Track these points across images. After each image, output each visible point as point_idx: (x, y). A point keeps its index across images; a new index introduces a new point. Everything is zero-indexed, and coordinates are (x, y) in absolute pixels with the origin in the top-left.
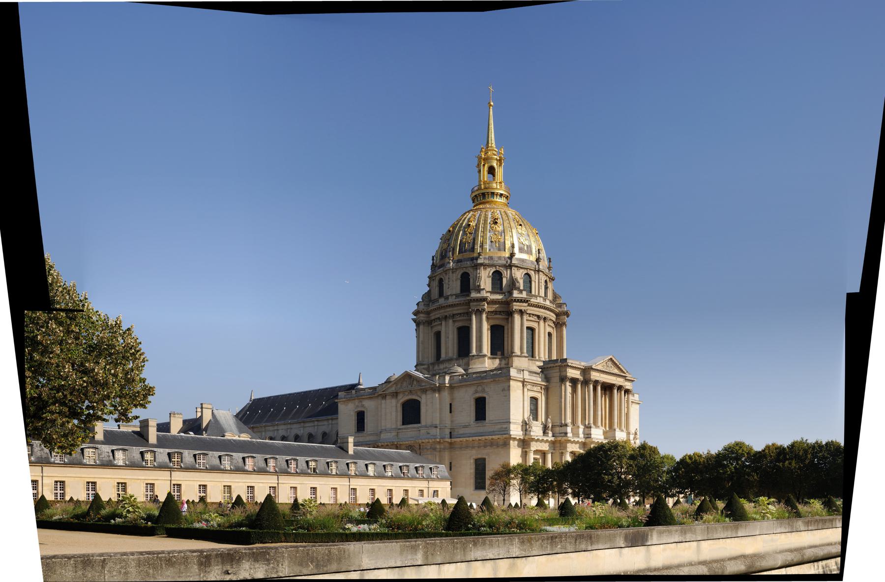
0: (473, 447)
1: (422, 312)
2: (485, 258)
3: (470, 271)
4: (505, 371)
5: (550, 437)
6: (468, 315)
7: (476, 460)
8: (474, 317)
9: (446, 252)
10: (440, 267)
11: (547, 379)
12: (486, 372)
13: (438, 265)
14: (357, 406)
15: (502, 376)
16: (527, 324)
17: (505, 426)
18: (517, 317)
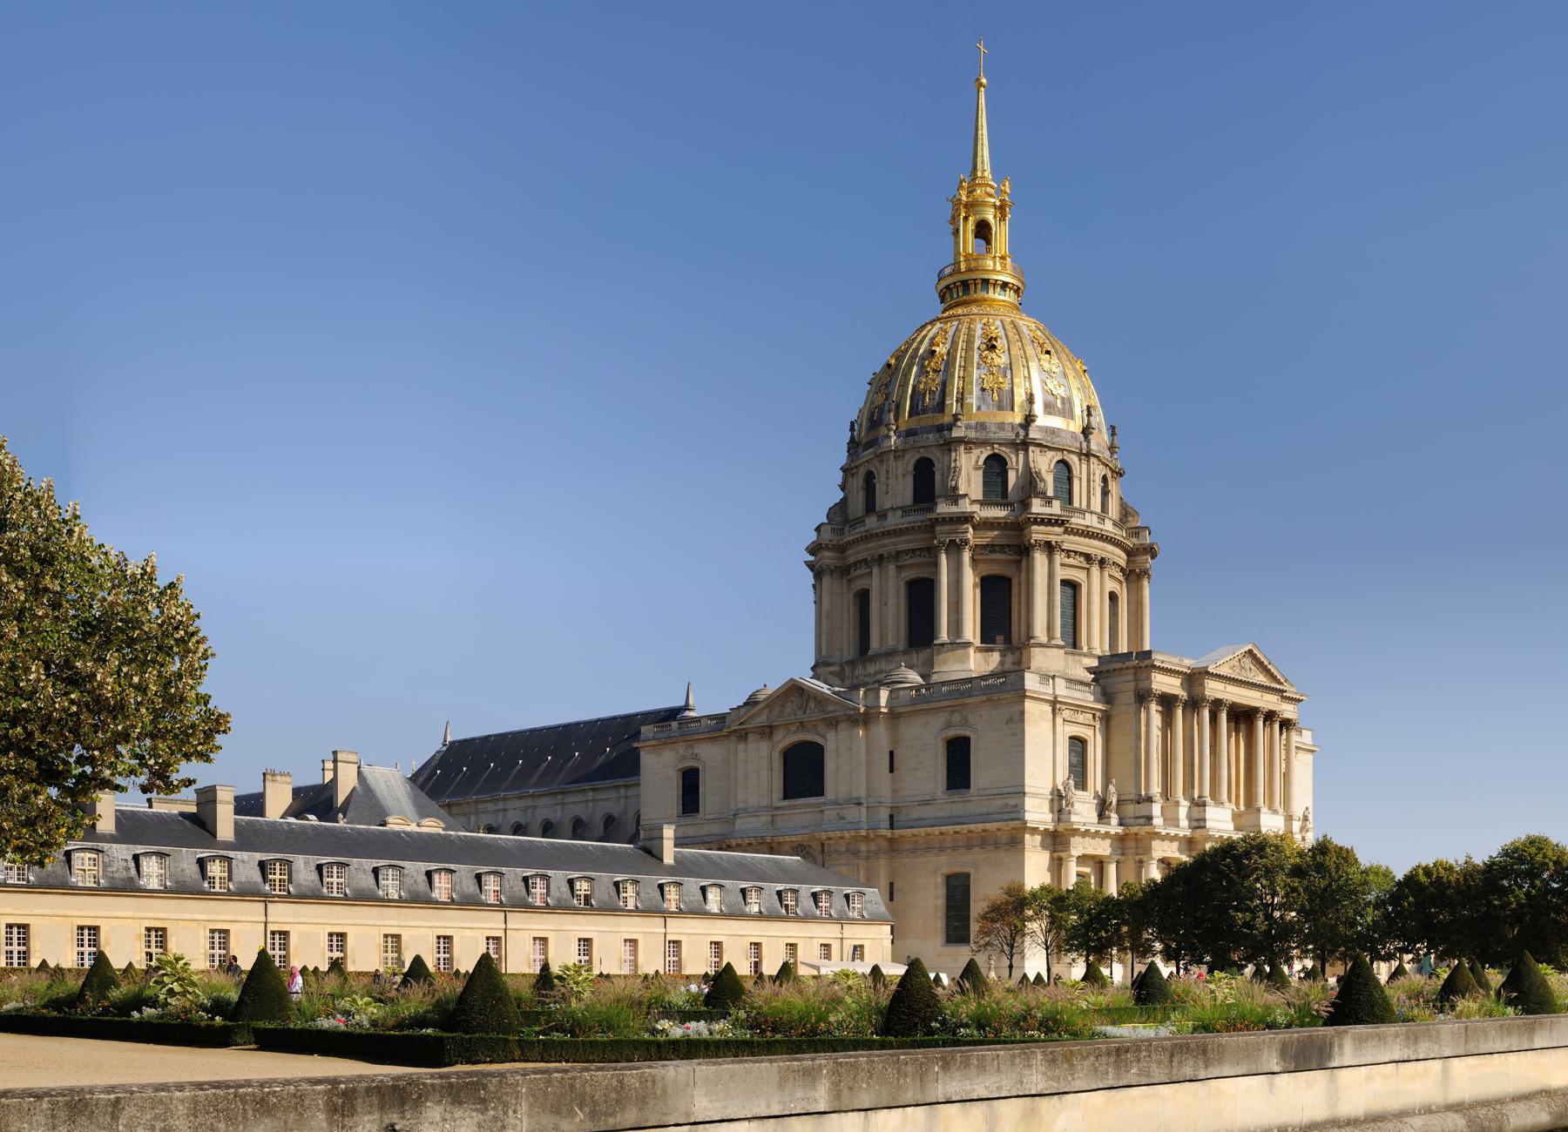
0: (942, 849)
1: (827, 548)
2: (968, 427)
3: (935, 455)
4: (1012, 677)
5: (1114, 827)
6: (932, 552)
8: (943, 558)
9: (881, 412)
10: (869, 445)
11: (1107, 696)
12: (970, 680)
13: (864, 442)
14: (683, 758)
15: (1006, 690)
16: (1061, 574)
17: (1012, 802)
18: (1040, 559)
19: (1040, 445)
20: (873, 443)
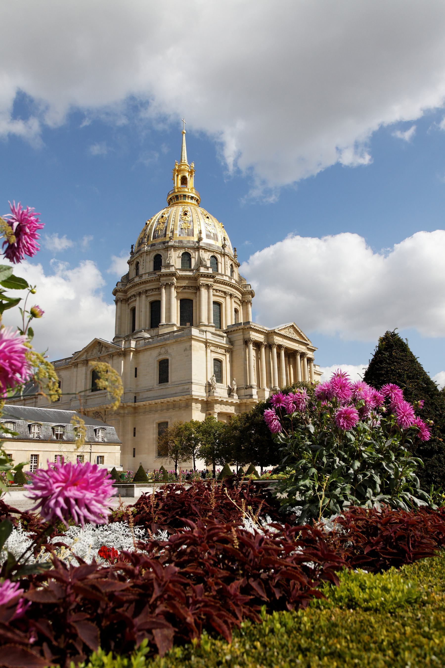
0: (156, 411)
3: (162, 253)
5: (235, 399)
6: (159, 289)
7: (159, 425)
8: (164, 291)
17: (187, 387)
18: (204, 291)
19: (204, 249)
20: (140, 250)
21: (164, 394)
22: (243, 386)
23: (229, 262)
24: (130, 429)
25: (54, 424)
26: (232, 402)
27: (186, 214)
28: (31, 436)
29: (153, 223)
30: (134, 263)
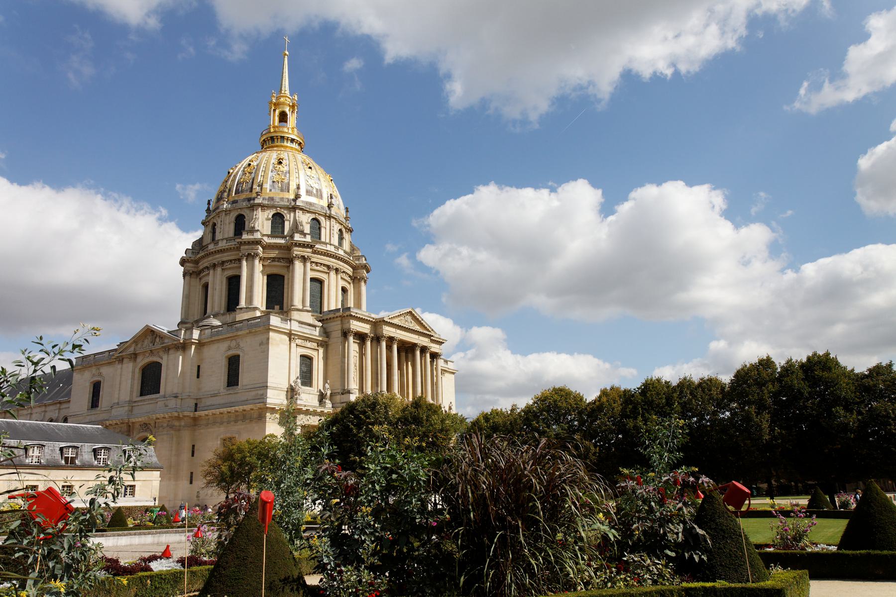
0: (222, 423)
3: (245, 213)
6: (239, 260)
8: (244, 263)
16: (311, 274)
17: (260, 392)
18: (298, 266)
19: (302, 209)
20: (217, 208)
21: (233, 400)
22: (339, 391)
23: (337, 227)
24: (187, 446)
25: (63, 445)
26: (322, 411)
27: (280, 163)
28: (28, 461)
29: (238, 172)
30: (210, 225)
